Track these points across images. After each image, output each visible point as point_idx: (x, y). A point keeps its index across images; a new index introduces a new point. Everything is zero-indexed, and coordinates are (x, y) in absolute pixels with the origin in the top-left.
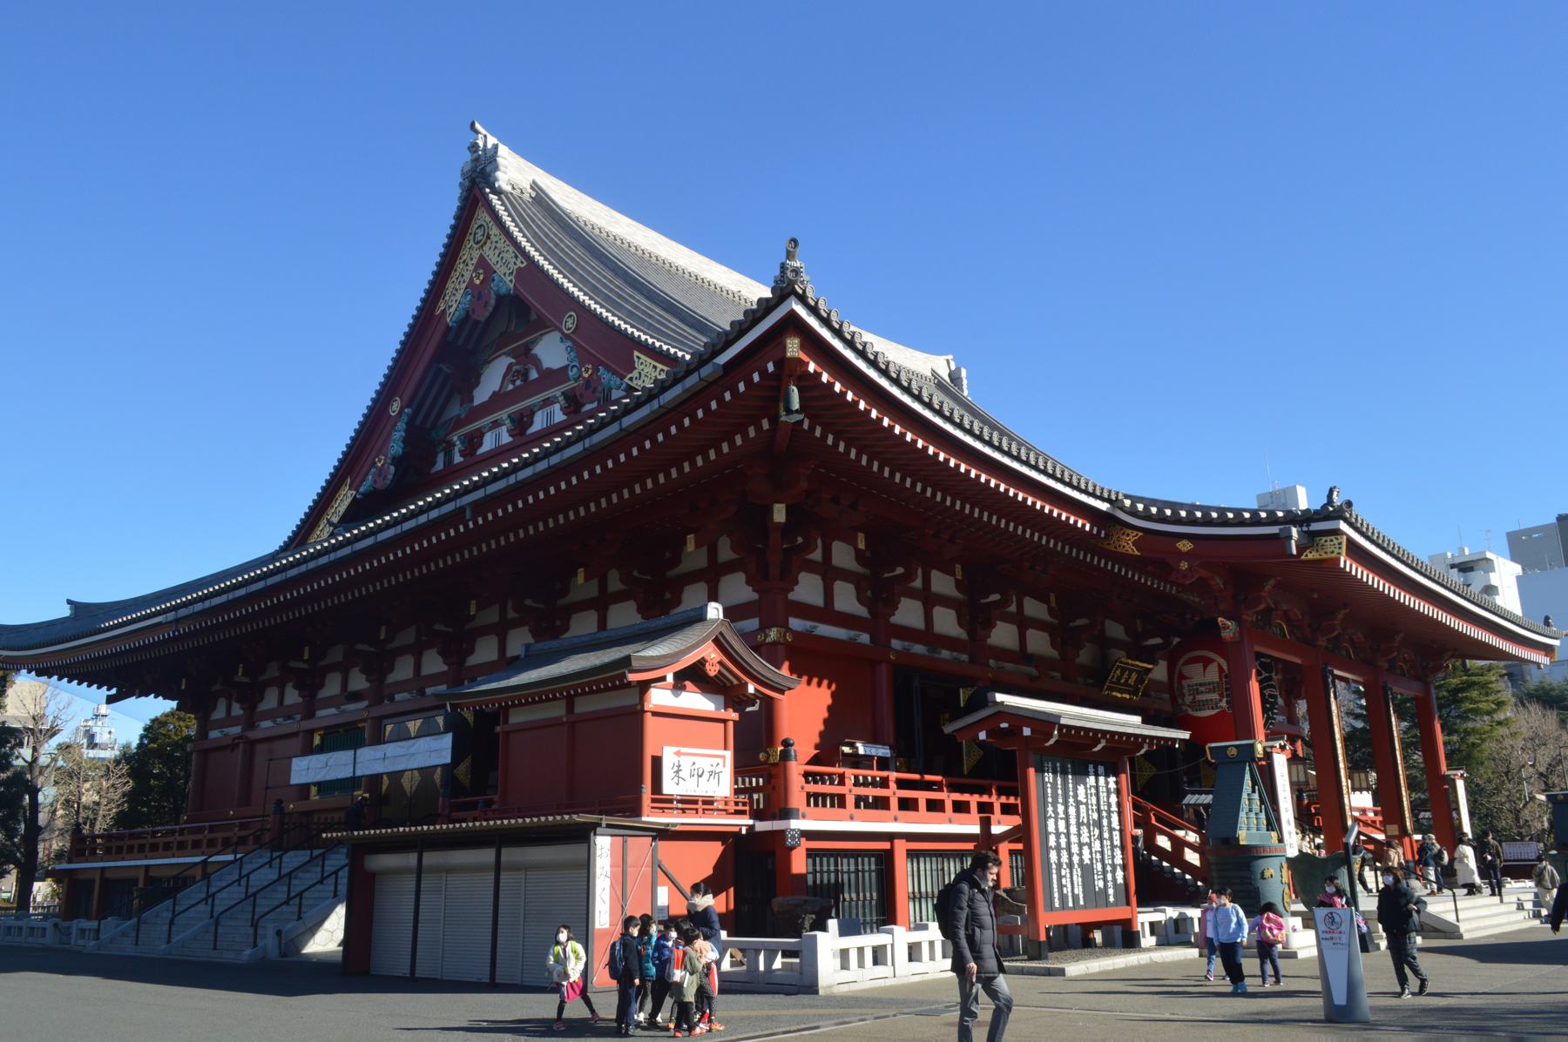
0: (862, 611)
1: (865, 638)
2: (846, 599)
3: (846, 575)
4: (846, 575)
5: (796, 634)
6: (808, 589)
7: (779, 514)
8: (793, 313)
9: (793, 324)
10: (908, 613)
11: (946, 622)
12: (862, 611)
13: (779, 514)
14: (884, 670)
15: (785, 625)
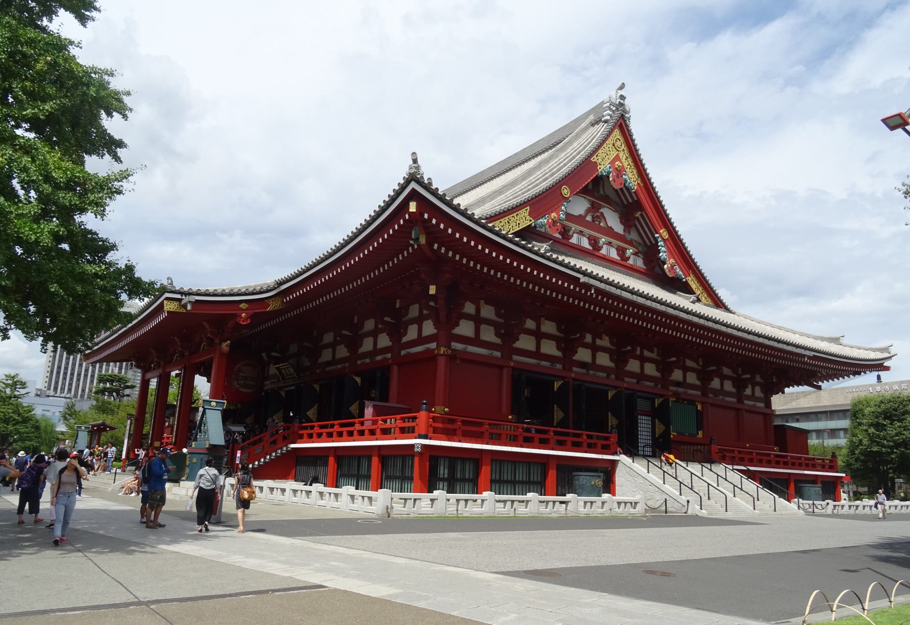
0: (498, 341)
1: (498, 354)
2: (488, 334)
3: (488, 322)
4: (488, 322)
5: (453, 350)
6: (465, 328)
7: (432, 290)
8: (413, 190)
9: (414, 195)
10: (526, 343)
11: (549, 348)
12: (498, 341)
13: (432, 290)
14: (506, 373)
15: (449, 347)
